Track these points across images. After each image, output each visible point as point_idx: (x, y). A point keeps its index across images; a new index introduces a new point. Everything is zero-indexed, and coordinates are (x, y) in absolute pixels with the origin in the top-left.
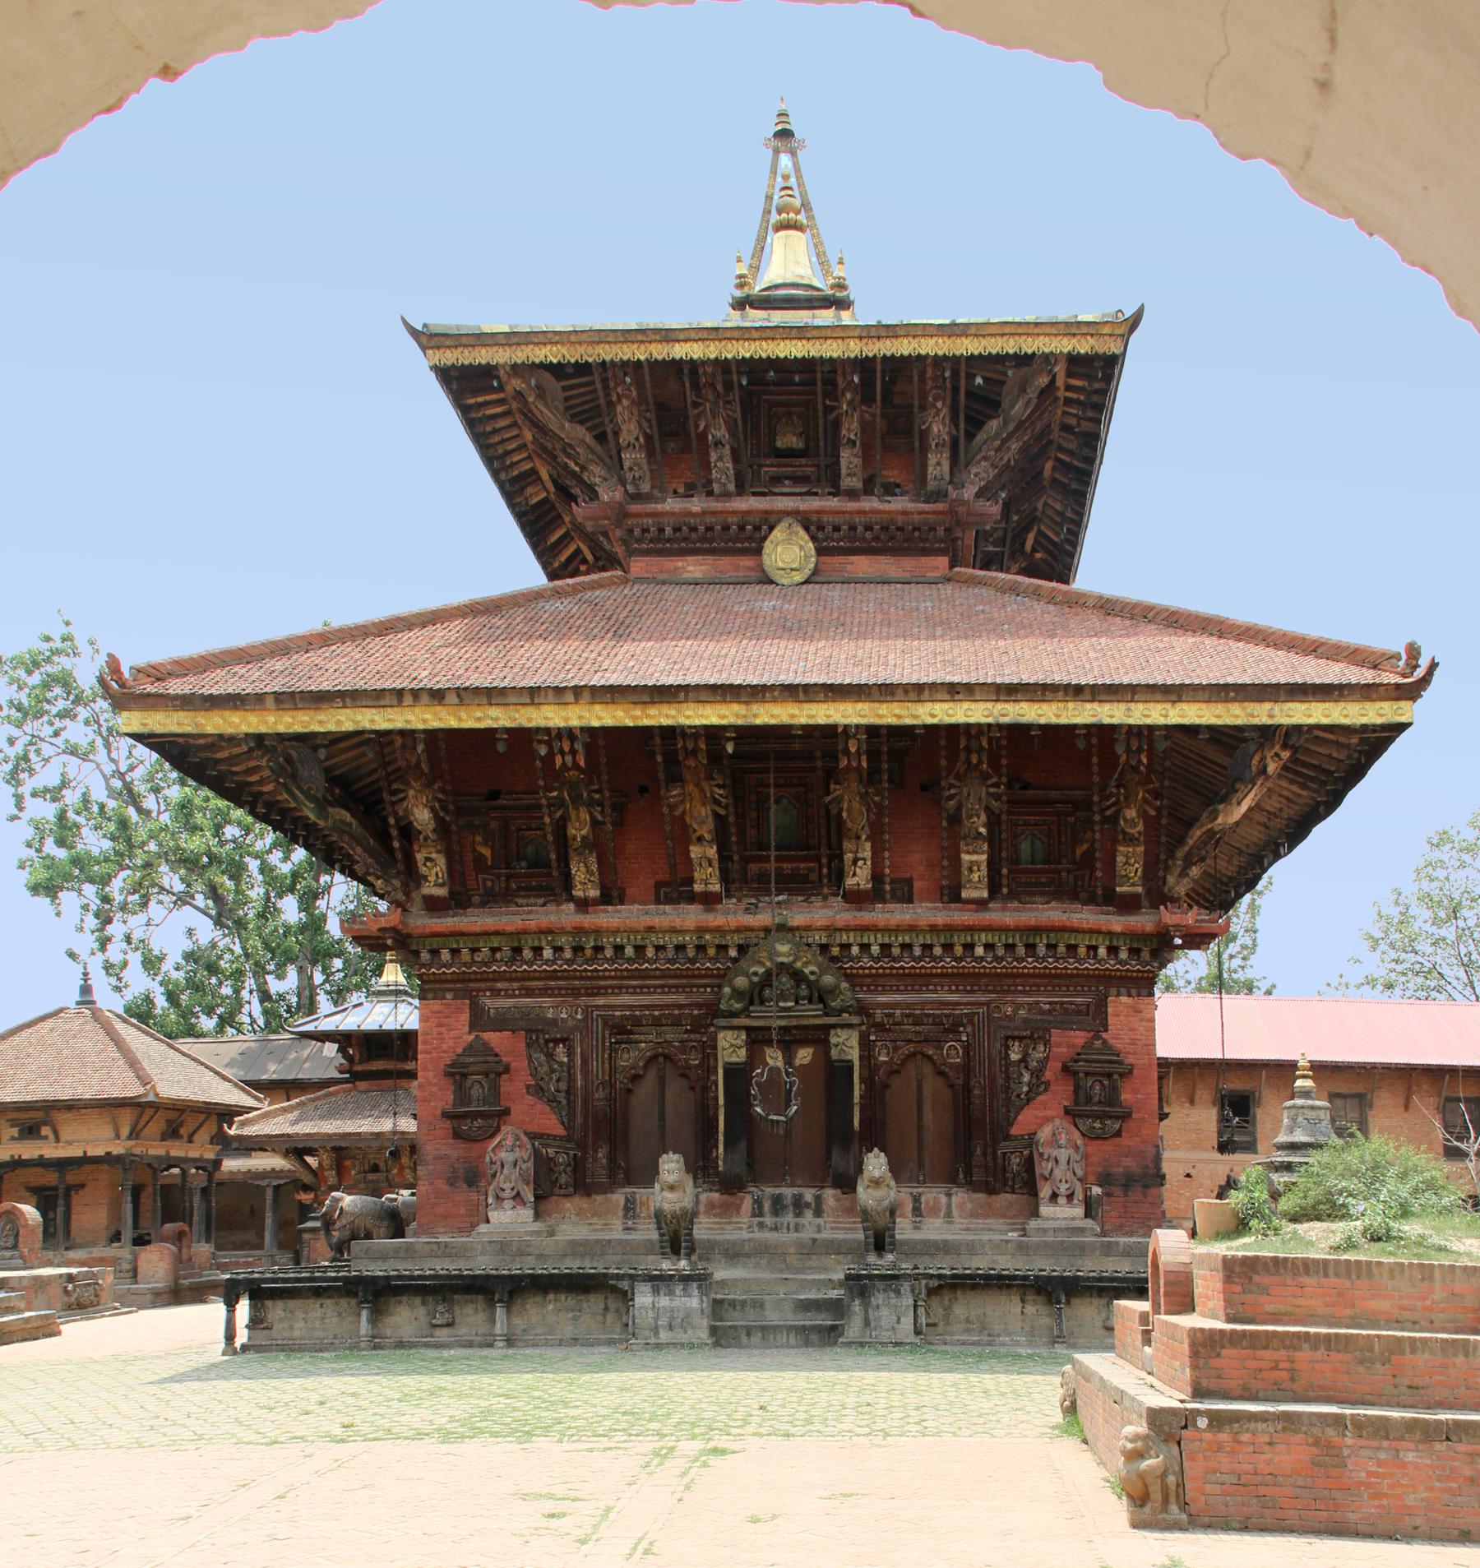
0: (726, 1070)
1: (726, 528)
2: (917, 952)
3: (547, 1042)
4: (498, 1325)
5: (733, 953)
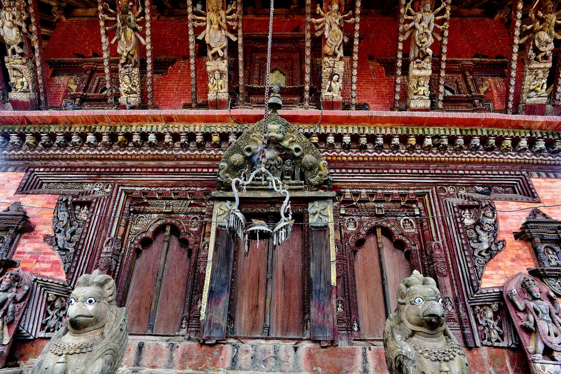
0: (218, 231)
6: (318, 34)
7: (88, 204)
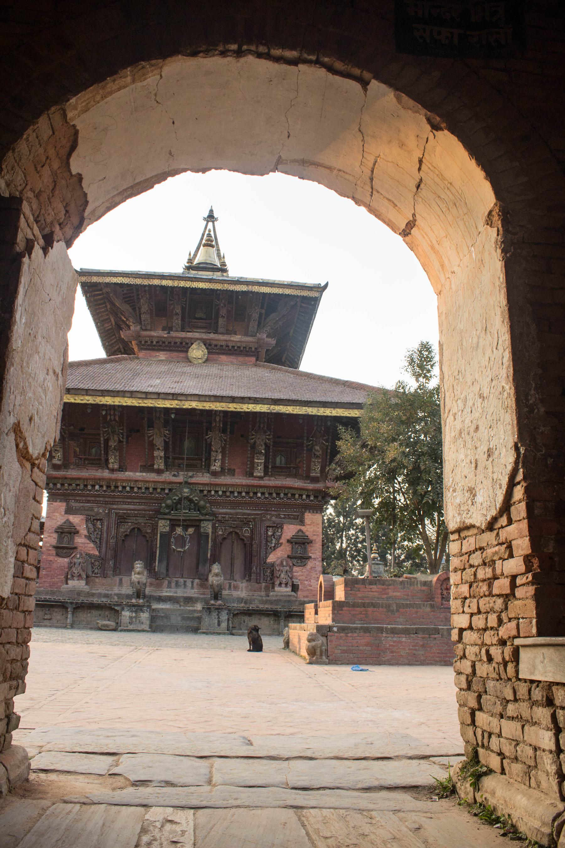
0: (161, 534)
1: (176, 343)
2: (236, 494)
3: (94, 520)
4: (69, 620)
5: (167, 491)
6: (208, 442)
7: (100, 520)
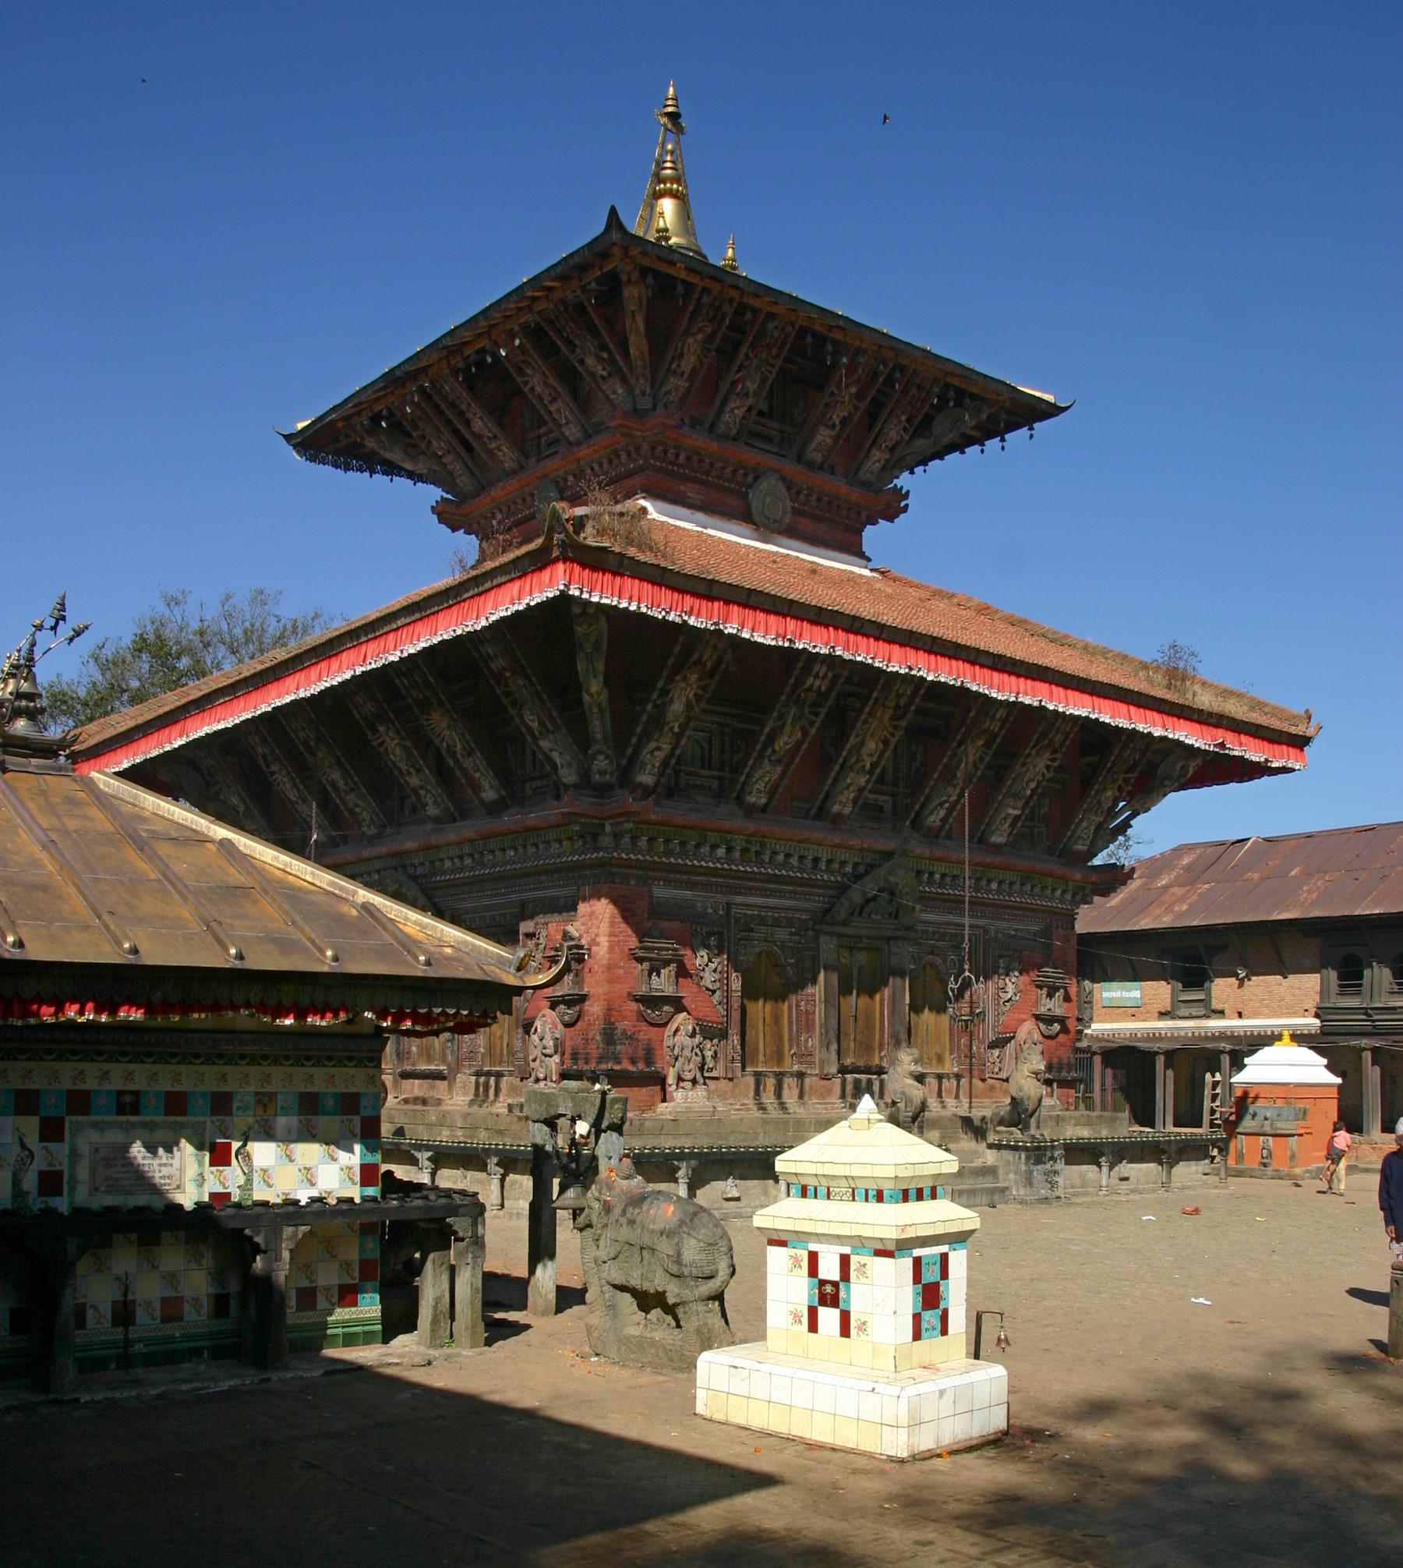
5: (849, 869)
